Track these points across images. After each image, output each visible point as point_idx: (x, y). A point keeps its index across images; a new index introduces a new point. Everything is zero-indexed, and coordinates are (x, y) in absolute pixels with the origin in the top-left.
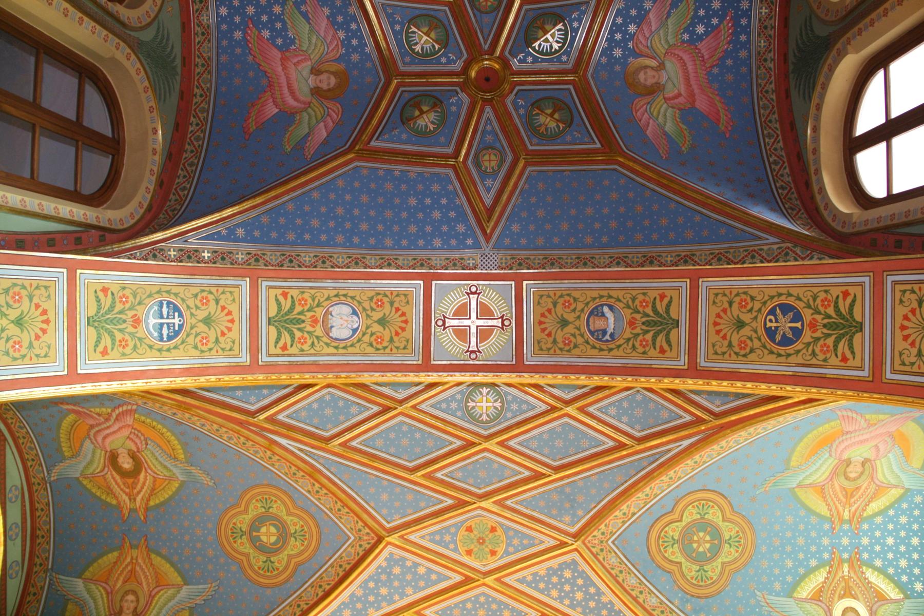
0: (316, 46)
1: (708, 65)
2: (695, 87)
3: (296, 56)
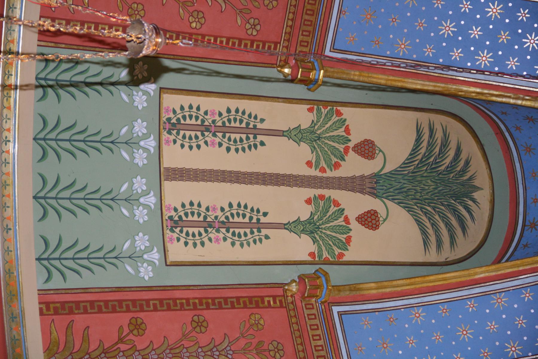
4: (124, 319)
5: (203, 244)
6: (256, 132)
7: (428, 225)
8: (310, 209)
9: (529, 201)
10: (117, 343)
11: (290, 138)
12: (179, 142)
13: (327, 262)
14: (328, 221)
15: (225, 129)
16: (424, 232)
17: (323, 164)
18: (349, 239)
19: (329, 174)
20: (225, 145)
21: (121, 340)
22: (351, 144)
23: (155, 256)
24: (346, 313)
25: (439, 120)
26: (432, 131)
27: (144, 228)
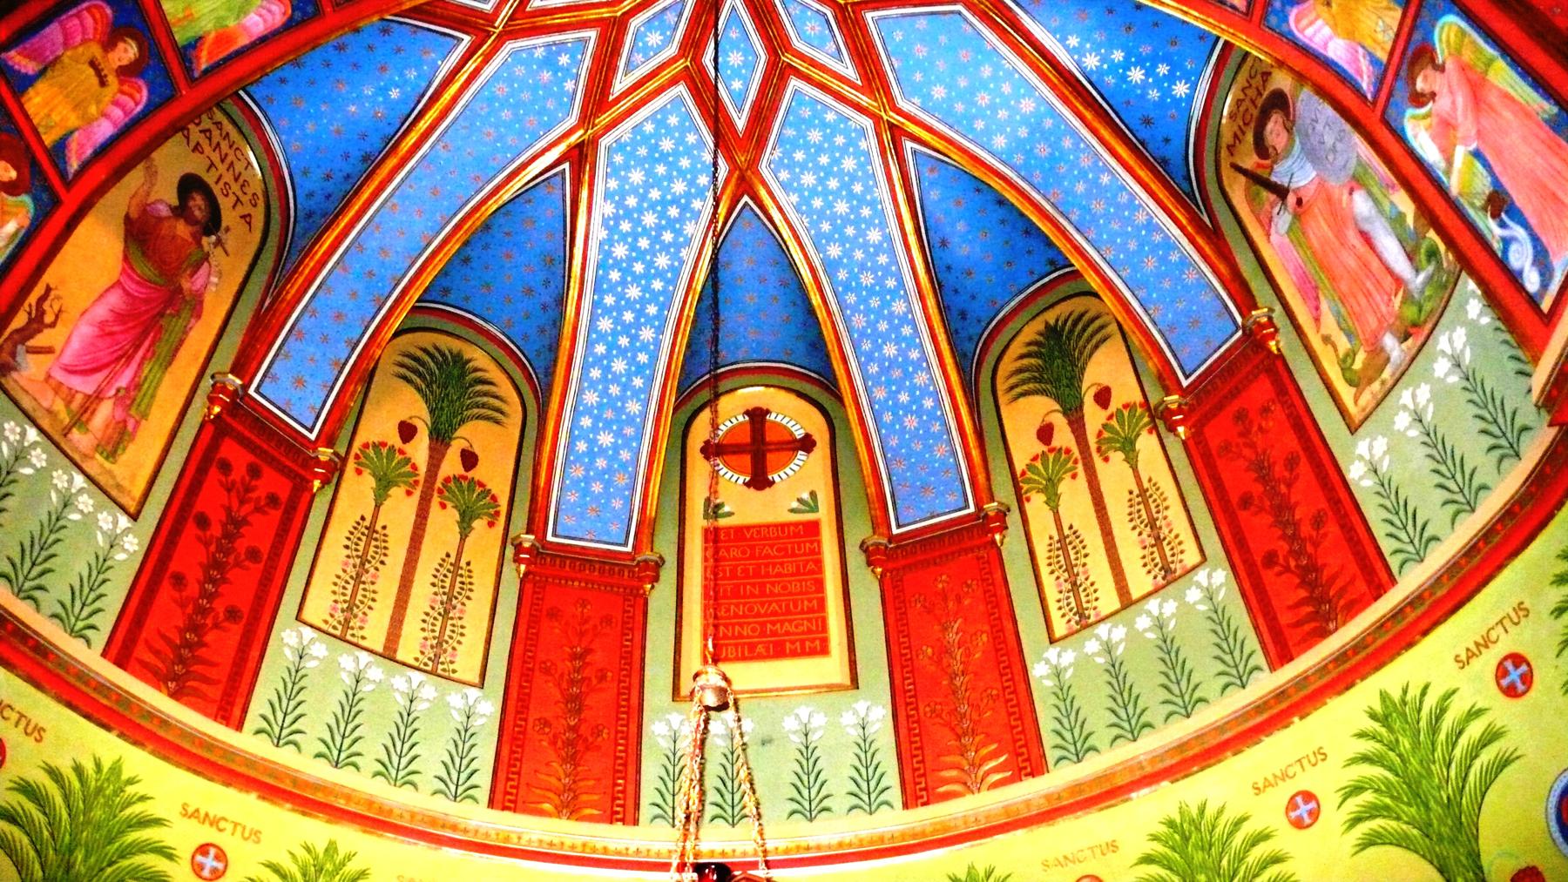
4: (1268, 576)
5: (1177, 536)
6: (1062, 538)
7: (1089, 346)
8: (1111, 454)
9: (1036, 277)
10: (1292, 572)
11: (1058, 505)
12: (1095, 604)
13: (1152, 418)
14: (1118, 433)
15: (1070, 568)
16: (1096, 347)
17: (1070, 464)
19: (1076, 453)
20: (1083, 560)
21: (1287, 569)
22: (1045, 448)
23: (1201, 576)
24: (1184, 373)
26: (1012, 388)
27: (1181, 598)
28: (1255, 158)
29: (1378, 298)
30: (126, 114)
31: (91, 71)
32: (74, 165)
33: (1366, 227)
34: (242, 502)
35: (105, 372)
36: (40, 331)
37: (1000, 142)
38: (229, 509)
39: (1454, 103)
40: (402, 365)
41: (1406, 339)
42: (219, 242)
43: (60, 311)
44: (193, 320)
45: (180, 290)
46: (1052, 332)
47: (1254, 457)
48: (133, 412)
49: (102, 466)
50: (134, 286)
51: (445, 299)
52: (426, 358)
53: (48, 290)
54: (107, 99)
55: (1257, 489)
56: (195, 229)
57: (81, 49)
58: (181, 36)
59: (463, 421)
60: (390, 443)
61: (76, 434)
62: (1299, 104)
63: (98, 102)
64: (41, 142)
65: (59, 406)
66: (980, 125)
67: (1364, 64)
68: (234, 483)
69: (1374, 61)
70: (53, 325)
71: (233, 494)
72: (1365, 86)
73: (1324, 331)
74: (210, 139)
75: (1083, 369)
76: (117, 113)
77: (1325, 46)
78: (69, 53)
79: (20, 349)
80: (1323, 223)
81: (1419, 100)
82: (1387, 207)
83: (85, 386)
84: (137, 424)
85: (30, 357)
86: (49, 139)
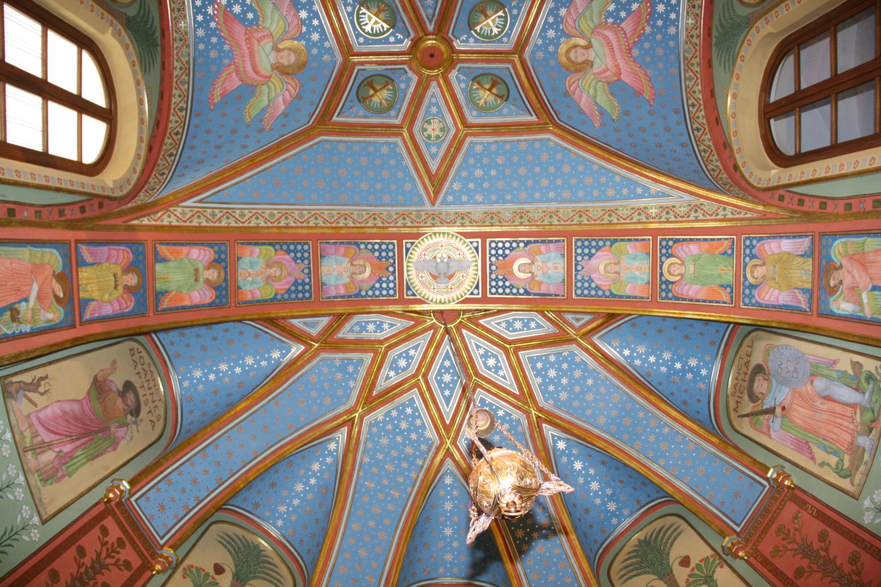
0: (590, 86)
1: (233, 67)
2: (245, 47)
3: (607, 77)
16: (675, 539)
18: (701, 561)
25: (614, 578)
28: (752, 404)
29: (846, 423)
30: (120, 309)
31: (113, 279)
32: (87, 316)
33: (826, 394)
34: (108, 556)
35: (58, 437)
36: (35, 392)
37: (602, 420)
38: (99, 555)
39: (853, 276)
40: (222, 538)
41: (870, 432)
42: (135, 423)
43: (48, 390)
44: (110, 448)
45: (108, 428)
46: (644, 543)
47: (797, 547)
48: (64, 467)
49: (36, 481)
50: (88, 410)
51: (254, 511)
52: (237, 540)
53: (46, 377)
54: (115, 296)
55: (805, 563)
56: (126, 408)
57: (112, 266)
58: (159, 286)
59: (255, 578)
60: (207, 571)
61: (30, 455)
62: (770, 363)
63: (110, 295)
64: (79, 294)
65: (28, 434)
66: (589, 412)
67: (800, 297)
68: (107, 542)
69: (804, 291)
70: (42, 394)
71: (105, 548)
72: (804, 306)
73: (819, 461)
74: (146, 375)
75: (668, 554)
76: (117, 306)
77: (778, 299)
78: (107, 264)
79: (21, 392)
80: (800, 409)
81: (833, 291)
82: (834, 374)
83: (47, 437)
84: (63, 476)
85: (24, 400)
86: (82, 295)
